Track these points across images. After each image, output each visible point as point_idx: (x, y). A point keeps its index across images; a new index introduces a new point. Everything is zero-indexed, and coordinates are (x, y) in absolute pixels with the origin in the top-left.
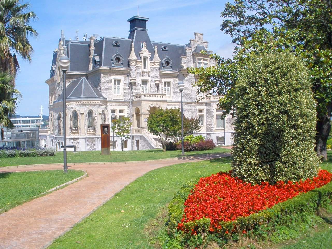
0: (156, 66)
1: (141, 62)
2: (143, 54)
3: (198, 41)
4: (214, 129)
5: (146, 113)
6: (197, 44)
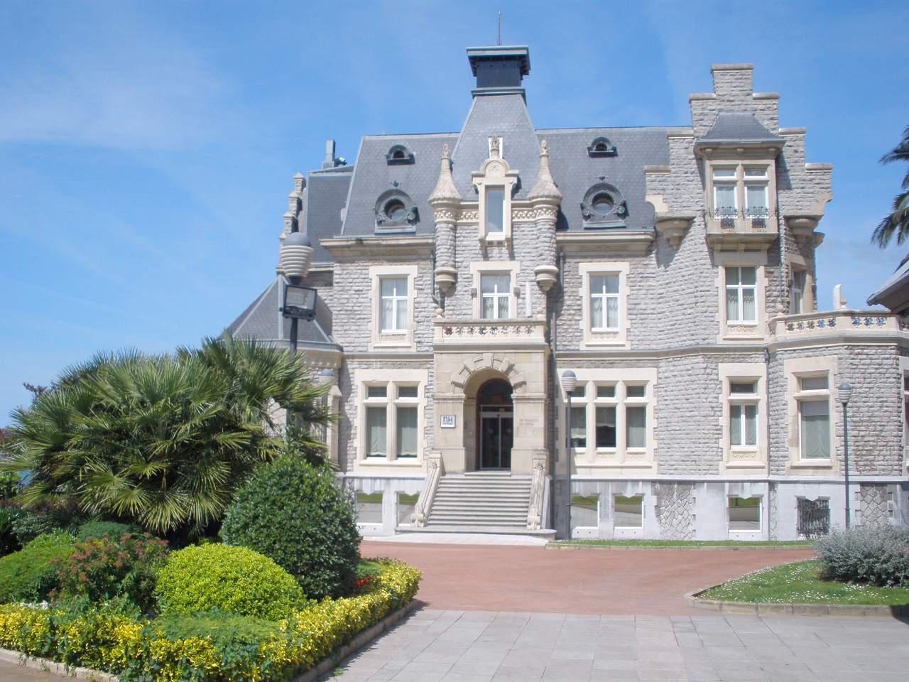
0: (541, 217)
1: (476, 207)
2: (483, 176)
3: (726, 98)
4: (788, 464)
5: (449, 394)
6: (720, 110)
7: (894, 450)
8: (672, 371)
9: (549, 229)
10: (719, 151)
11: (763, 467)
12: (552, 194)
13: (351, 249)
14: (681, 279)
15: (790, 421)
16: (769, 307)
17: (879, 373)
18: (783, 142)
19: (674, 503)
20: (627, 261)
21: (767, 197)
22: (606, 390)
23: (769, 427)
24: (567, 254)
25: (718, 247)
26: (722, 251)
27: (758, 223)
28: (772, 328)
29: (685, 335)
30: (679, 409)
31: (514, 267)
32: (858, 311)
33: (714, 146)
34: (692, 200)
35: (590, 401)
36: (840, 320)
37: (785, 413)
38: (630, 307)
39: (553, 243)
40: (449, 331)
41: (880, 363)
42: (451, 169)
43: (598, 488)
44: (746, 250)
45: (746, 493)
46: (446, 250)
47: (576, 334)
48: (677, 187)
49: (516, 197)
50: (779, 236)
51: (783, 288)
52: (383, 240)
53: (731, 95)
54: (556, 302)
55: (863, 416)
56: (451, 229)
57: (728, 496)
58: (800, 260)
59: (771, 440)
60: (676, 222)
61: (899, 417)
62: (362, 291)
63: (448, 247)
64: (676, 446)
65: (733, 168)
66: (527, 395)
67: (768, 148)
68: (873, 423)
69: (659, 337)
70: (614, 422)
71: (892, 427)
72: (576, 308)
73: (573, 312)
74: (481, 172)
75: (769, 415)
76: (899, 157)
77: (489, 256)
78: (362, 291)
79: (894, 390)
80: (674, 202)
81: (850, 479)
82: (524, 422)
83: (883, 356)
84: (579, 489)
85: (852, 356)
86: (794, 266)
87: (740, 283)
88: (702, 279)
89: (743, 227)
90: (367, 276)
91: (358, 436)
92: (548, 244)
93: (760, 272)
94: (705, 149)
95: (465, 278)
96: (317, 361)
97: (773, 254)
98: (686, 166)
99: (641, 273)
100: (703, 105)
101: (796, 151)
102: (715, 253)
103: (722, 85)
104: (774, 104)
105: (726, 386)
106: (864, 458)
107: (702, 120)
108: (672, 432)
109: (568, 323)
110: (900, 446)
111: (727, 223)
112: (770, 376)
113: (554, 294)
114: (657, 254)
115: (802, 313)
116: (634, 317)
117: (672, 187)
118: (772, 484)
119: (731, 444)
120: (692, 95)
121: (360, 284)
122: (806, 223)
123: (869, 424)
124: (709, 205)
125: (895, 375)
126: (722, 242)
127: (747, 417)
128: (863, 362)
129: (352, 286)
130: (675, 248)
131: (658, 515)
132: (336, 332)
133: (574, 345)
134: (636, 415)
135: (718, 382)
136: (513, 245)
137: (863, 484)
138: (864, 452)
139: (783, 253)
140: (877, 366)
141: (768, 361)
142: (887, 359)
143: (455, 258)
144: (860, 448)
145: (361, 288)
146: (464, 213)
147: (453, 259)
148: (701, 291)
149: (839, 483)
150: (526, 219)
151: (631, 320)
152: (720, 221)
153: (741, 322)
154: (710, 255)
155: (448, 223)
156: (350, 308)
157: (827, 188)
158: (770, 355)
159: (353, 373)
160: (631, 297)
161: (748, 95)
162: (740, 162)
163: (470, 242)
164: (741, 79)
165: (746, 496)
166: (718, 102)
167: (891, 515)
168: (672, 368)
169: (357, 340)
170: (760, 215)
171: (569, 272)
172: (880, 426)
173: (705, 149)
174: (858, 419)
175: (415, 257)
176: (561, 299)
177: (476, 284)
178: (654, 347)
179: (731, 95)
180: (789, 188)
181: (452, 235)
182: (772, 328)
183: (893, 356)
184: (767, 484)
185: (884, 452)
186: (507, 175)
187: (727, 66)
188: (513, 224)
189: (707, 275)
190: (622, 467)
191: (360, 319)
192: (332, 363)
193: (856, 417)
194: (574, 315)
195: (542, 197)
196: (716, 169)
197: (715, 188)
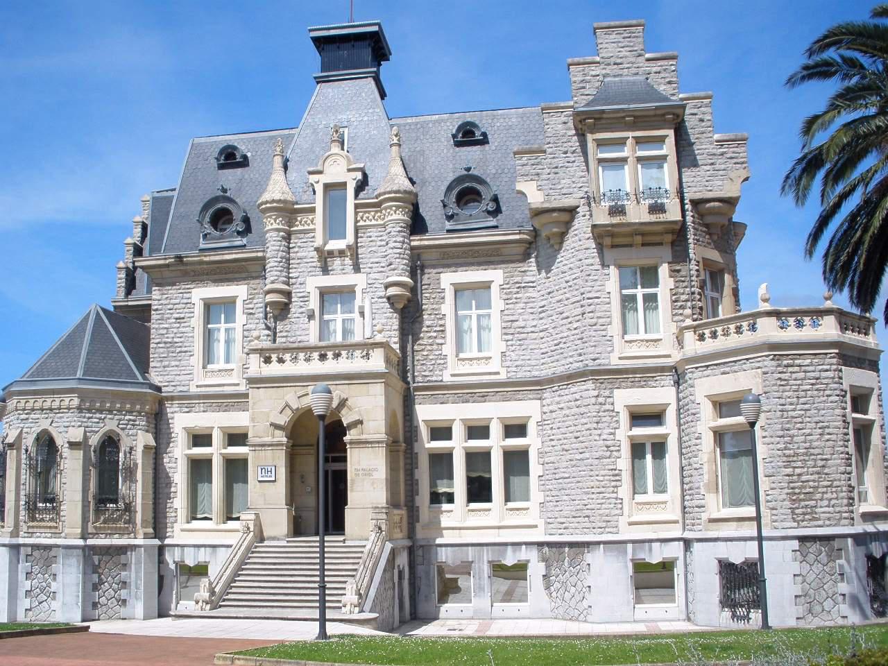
0: (390, 218)
1: (312, 210)
2: (320, 172)
3: (612, 60)
4: (705, 516)
5: (268, 439)
7: (842, 492)
8: (558, 403)
9: (399, 232)
10: (603, 122)
11: (676, 522)
12: (402, 188)
13: (170, 269)
14: (565, 285)
15: (705, 459)
16: (676, 315)
17: (817, 390)
18: (684, 107)
19: (566, 571)
20: (500, 268)
21: (667, 176)
22: (478, 430)
23: (682, 469)
24: (427, 263)
25: (607, 241)
26: (613, 246)
27: (657, 208)
28: (680, 342)
29: (571, 356)
30: (566, 451)
31: (359, 280)
32: (784, 309)
34: (574, 186)
35: (458, 445)
36: (762, 322)
37: (698, 450)
38: (504, 325)
39: (405, 249)
40: (268, 360)
41: (818, 376)
42: (286, 168)
43: (471, 553)
44: (643, 245)
45: (656, 555)
46: (276, 264)
47: (439, 361)
48: (553, 170)
49: (362, 195)
50: (684, 222)
51: (693, 289)
52: (205, 256)
53: (618, 57)
54: (413, 322)
55: (798, 448)
56: (283, 238)
57: (632, 560)
58: (715, 255)
59: (685, 486)
60: (555, 214)
61: (847, 447)
62: (183, 318)
63: (279, 260)
64: (565, 498)
65: (622, 142)
66: (364, 437)
67: (664, 115)
68: (813, 457)
69: (542, 361)
70: (490, 471)
71: (837, 462)
72: (438, 329)
73: (435, 334)
74: (320, 168)
75: (681, 454)
76: (810, 77)
77: (330, 268)
78: (183, 318)
79: (838, 411)
80: (551, 189)
81: (764, 534)
82: (361, 473)
83: (821, 367)
84: (447, 557)
85: (780, 369)
86: (707, 263)
87: (639, 287)
88: (589, 284)
89: (638, 214)
90: (189, 301)
91: (179, 494)
92: (399, 251)
93: (664, 270)
94: (585, 120)
95: (300, 297)
97: (678, 248)
98: (565, 145)
99: (517, 283)
100: (583, 70)
101: (702, 120)
102: (605, 250)
103: (607, 45)
104: (672, 65)
105: (624, 418)
106: (803, 504)
107: (584, 88)
108: (560, 481)
109: (429, 348)
110: (850, 486)
111: (617, 210)
112: (680, 403)
113: (410, 313)
114: (536, 257)
115: (721, 317)
116: (510, 337)
117: (548, 171)
118: (687, 543)
119: (634, 493)
120: (570, 60)
121: (181, 311)
122: (719, 207)
123: (807, 458)
124: (594, 188)
125: (838, 392)
126: (612, 235)
127: (654, 457)
128: (794, 376)
129: (172, 314)
130: (556, 247)
131: (547, 588)
132: (155, 369)
133: (437, 376)
134: (517, 462)
135: (614, 414)
136: (357, 254)
137: (802, 539)
138: (802, 496)
139: (692, 246)
140: (814, 381)
141: (677, 383)
142: (827, 371)
143: (289, 273)
144: (797, 491)
145: (182, 316)
146: (299, 219)
147: (285, 274)
148: (588, 299)
149: (751, 539)
150: (374, 222)
151: (508, 341)
152: (607, 207)
153: (642, 336)
154: (598, 253)
155: (278, 230)
156: (169, 340)
157: (743, 163)
158: (678, 374)
159: (172, 418)
160: (506, 312)
161: (640, 55)
162: (630, 134)
163: (305, 252)
164: (629, 37)
165: (655, 559)
166: (602, 67)
167: (842, 580)
168: (557, 399)
169: (177, 378)
170: (658, 198)
171: (429, 285)
172: (822, 460)
173: (585, 120)
174: (792, 451)
175: (244, 275)
176: (420, 319)
177: (314, 304)
178: (536, 373)
179: (618, 57)
180: (695, 164)
181: (284, 246)
182: (680, 342)
183: (834, 367)
184: (682, 543)
185: (829, 496)
186: (349, 170)
187: (612, 23)
188: (357, 230)
189: (596, 278)
190: (499, 528)
191: (180, 352)
192: (143, 405)
193: (790, 449)
194: (436, 337)
195: (390, 192)
196: (600, 144)
197: (600, 168)
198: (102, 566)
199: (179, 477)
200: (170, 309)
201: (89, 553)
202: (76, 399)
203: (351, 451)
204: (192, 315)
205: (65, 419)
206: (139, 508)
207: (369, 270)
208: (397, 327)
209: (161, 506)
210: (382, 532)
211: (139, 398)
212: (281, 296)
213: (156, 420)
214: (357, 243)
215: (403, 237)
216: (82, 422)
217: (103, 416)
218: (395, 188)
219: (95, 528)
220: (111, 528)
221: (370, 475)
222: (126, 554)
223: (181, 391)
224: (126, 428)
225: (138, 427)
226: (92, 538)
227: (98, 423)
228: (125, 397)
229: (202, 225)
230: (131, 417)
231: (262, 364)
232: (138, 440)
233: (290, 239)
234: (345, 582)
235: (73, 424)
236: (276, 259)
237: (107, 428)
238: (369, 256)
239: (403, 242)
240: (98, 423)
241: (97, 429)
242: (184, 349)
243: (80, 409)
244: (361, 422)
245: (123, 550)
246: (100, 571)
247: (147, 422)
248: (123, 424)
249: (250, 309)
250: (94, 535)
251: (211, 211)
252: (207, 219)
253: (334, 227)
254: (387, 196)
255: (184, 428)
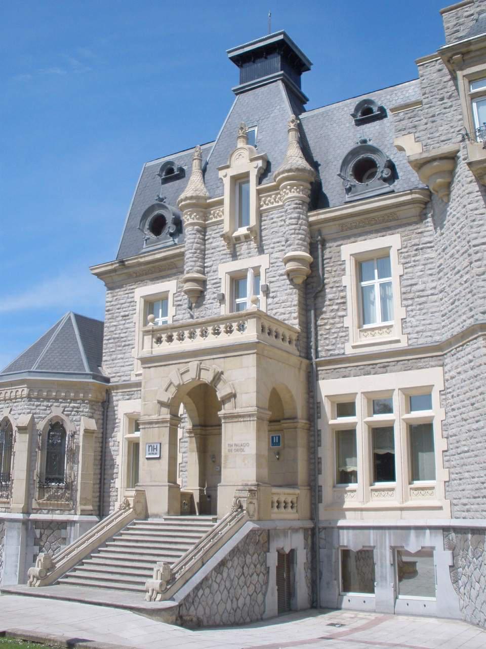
0: (286, 197)
1: (221, 203)
2: (228, 167)
5: (155, 417)
8: (457, 367)
9: (295, 208)
10: (472, 55)
12: (294, 167)
13: (117, 273)
14: (455, 237)
20: (398, 233)
22: (382, 405)
24: (327, 237)
29: (464, 313)
30: (466, 420)
31: (263, 261)
33: (464, 50)
34: (453, 130)
35: (361, 421)
38: (404, 290)
39: (301, 225)
40: (159, 341)
42: (204, 171)
43: (372, 538)
46: (191, 255)
47: (341, 334)
48: (431, 119)
49: (264, 181)
52: (141, 257)
54: (316, 297)
56: (198, 231)
60: (436, 164)
62: (128, 316)
63: (193, 251)
66: (238, 410)
69: (443, 324)
70: (393, 448)
72: (339, 301)
73: (336, 307)
74: (228, 164)
77: (238, 254)
78: (128, 316)
80: (429, 138)
82: (234, 448)
84: (348, 541)
88: (474, 230)
90: (132, 300)
91: (119, 475)
92: (293, 227)
95: (214, 284)
96: (77, 393)
98: (441, 92)
99: (414, 245)
100: (456, 14)
108: (462, 455)
109: (331, 321)
113: (311, 288)
114: (433, 216)
116: (410, 302)
117: (425, 121)
121: (126, 309)
129: (120, 313)
130: (445, 200)
132: (106, 363)
133: (339, 349)
134: (421, 435)
136: (261, 237)
143: (204, 263)
145: (127, 313)
146: (212, 212)
147: (199, 264)
148: (474, 246)
150: (275, 204)
151: (407, 306)
154: (482, 195)
155: (193, 224)
156: (117, 336)
159: (117, 406)
160: (405, 277)
163: (216, 243)
166: (476, 5)
168: (456, 363)
169: (123, 369)
171: (331, 258)
173: (451, 57)
175: (174, 271)
176: (322, 293)
177: (225, 289)
178: (437, 338)
181: (199, 238)
186: (252, 160)
188: (260, 214)
189: (481, 222)
190: (402, 509)
191: (125, 346)
192: (86, 393)
194: (338, 310)
195: (283, 172)
197: (474, 105)
198: (44, 538)
199: (120, 458)
200: (118, 309)
201: (29, 526)
202: (26, 389)
203: (225, 427)
204: (134, 312)
205: (19, 408)
206: (79, 488)
207: (271, 250)
208: (296, 302)
209: (106, 486)
210: (242, 510)
211: (83, 387)
212: (196, 284)
213: (104, 408)
214: (261, 226)
215: (299, 213)
216: (31, 409)
217: (50, 404)
218: (288, 167)
219: (39, 504)
220: (53, 505)
221: (243, 450)
222: (66, 528)
223: (124, 381)
224: (70, 415)
225: (82, 414)
226: (36, 513)
227: (45, 410)
228: (69, 386)
229: (143, 232)
230: (75, 405)
231: (155, 345)
232: (80, 423)
233: (205, 232)
234: (155, 562)
235: (23, 411)
236: (190, 251)
237: (53, 414)
238: (271, 237)
239: (299, 218)
240: (45, 410)
241: (43, 416)
242: (127, 343)
243: (29, 398)
244: (234, 396)
245: (63, 525)
246: (42, 544)
247: (91, 408)
248: (67, 411)
249: (178, 301)
250: (37, 511)
251: (149, 219)
252: (147, 226)
253: (240, 216)
254: (281, 176)
255: (125, 414)
